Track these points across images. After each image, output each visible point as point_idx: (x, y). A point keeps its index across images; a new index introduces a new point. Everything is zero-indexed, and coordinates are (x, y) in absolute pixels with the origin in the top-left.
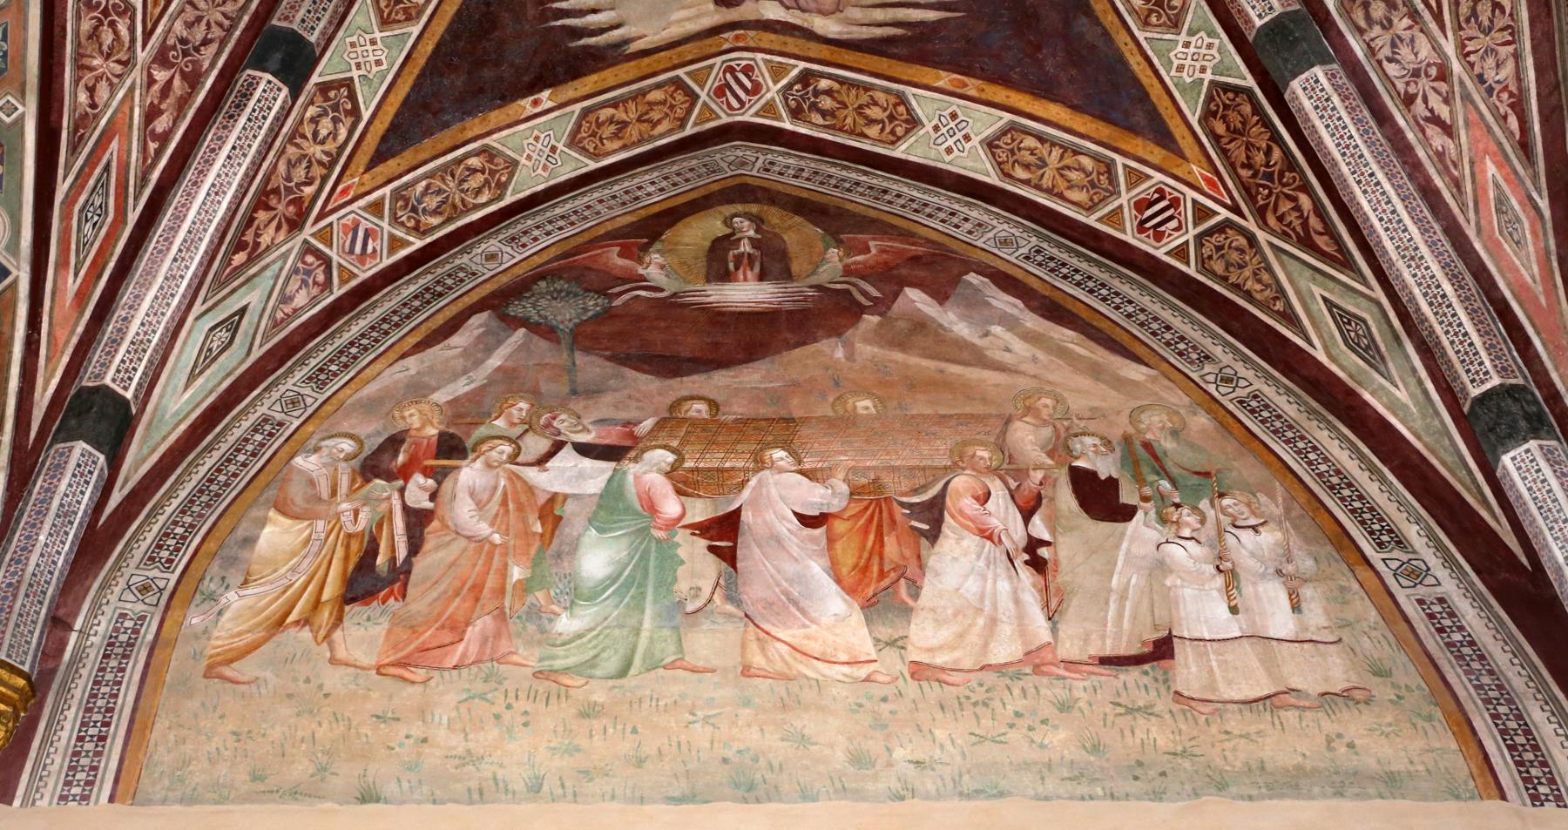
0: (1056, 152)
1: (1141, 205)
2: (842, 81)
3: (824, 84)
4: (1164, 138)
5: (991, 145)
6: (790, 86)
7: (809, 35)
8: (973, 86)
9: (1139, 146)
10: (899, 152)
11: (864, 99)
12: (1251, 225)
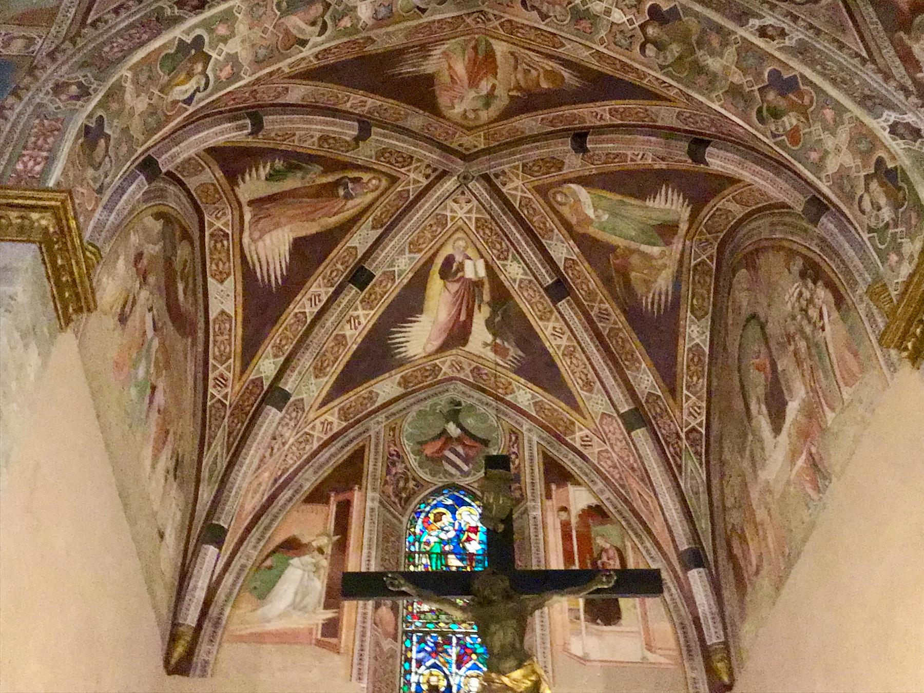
0: (227, 337)
1: (222, 376)
2: (228, 250)
3: (225, 243)
4: (243, 372)
5: (223, 312)
6: (222, 230)
7: (242, 231)
8: (240, 299)
9: (238, 364)
10: (210, 279)
11: (224, 260)
12: (228, 413)
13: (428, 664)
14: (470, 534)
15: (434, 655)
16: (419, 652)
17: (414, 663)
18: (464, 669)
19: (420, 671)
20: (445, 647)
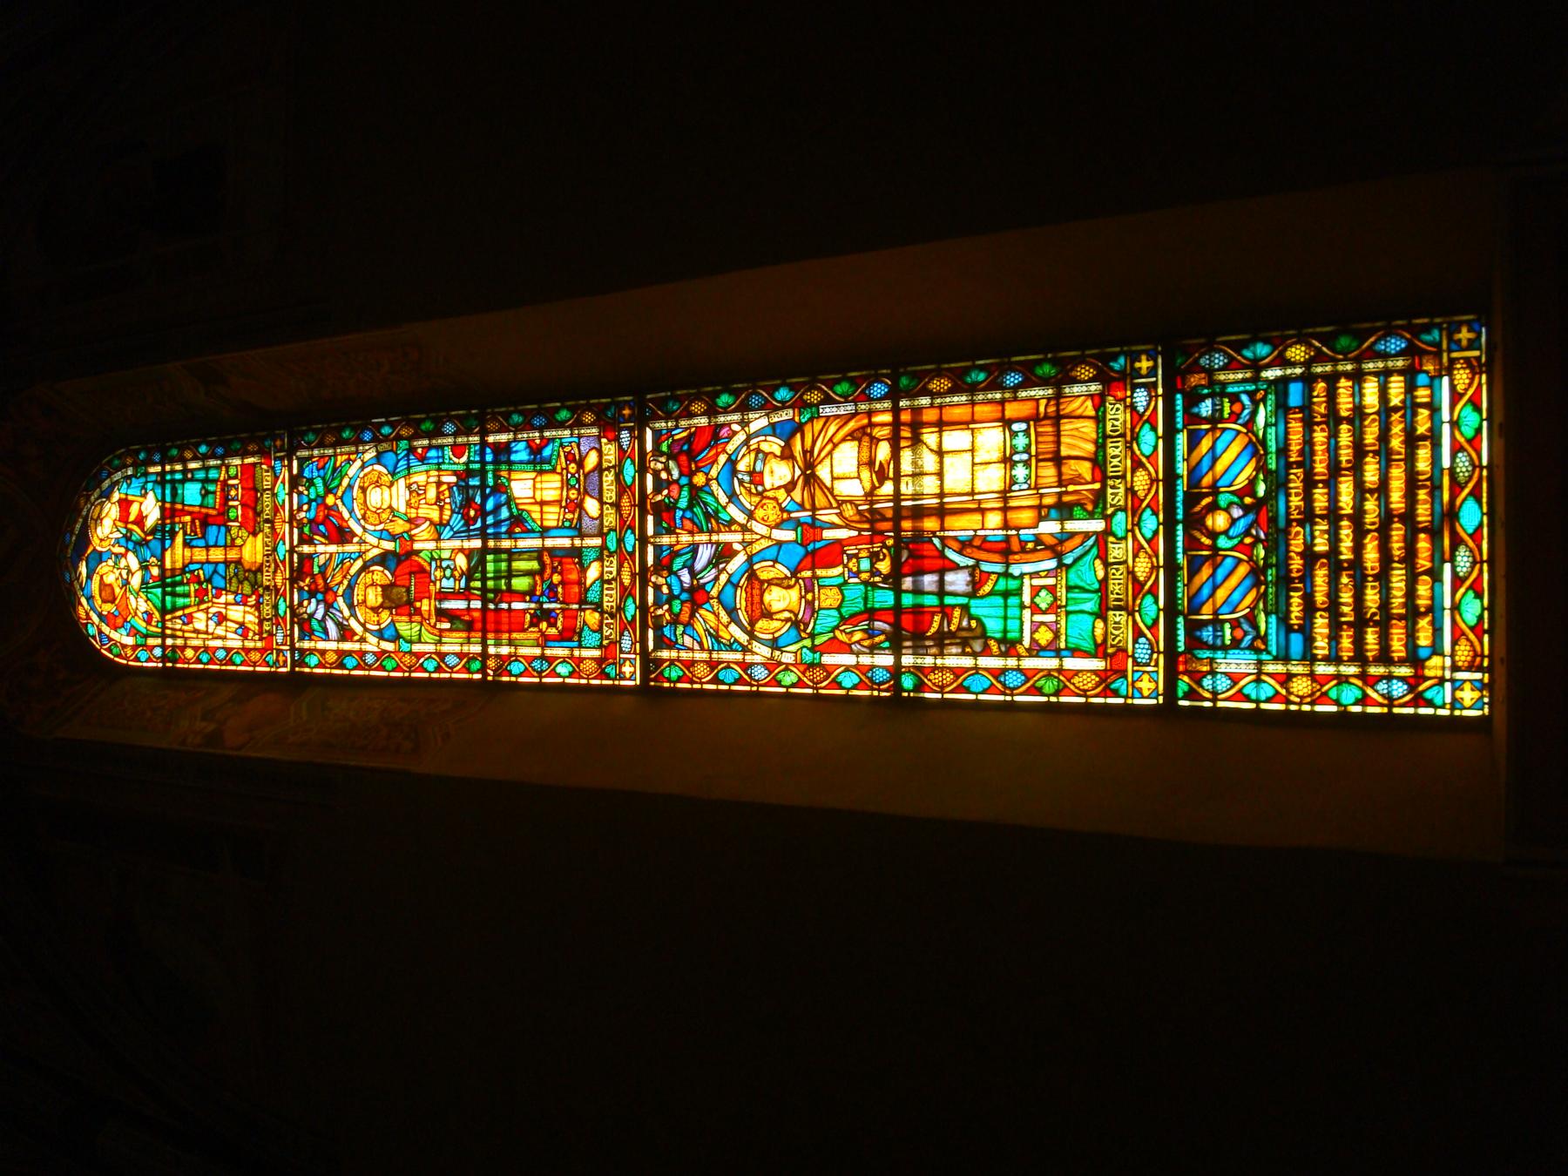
13: (347, 613)
14: (132, 518)
15: (330, 598)
16: (326, 631)
17: (347, 646)
18: (353, 524)
19: (358, 629)
20: (316, 570)
